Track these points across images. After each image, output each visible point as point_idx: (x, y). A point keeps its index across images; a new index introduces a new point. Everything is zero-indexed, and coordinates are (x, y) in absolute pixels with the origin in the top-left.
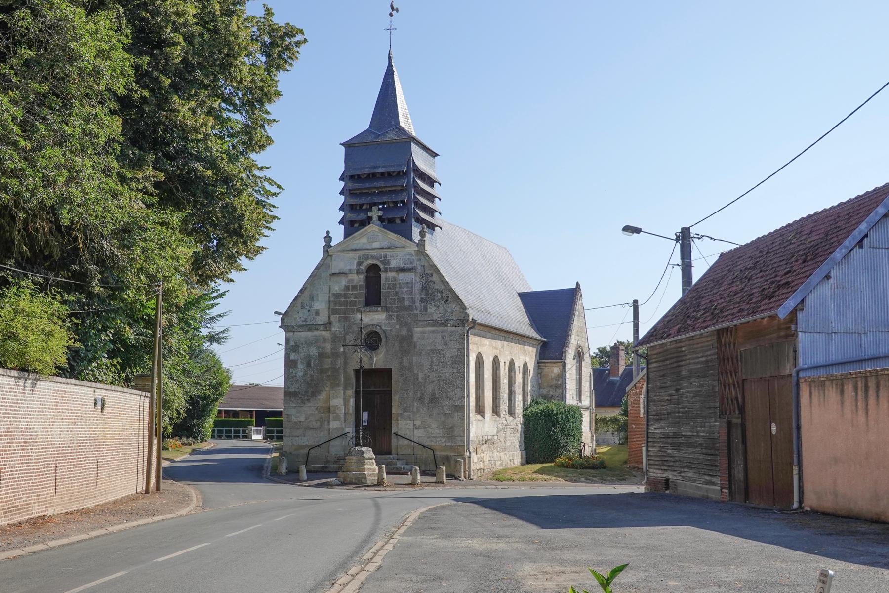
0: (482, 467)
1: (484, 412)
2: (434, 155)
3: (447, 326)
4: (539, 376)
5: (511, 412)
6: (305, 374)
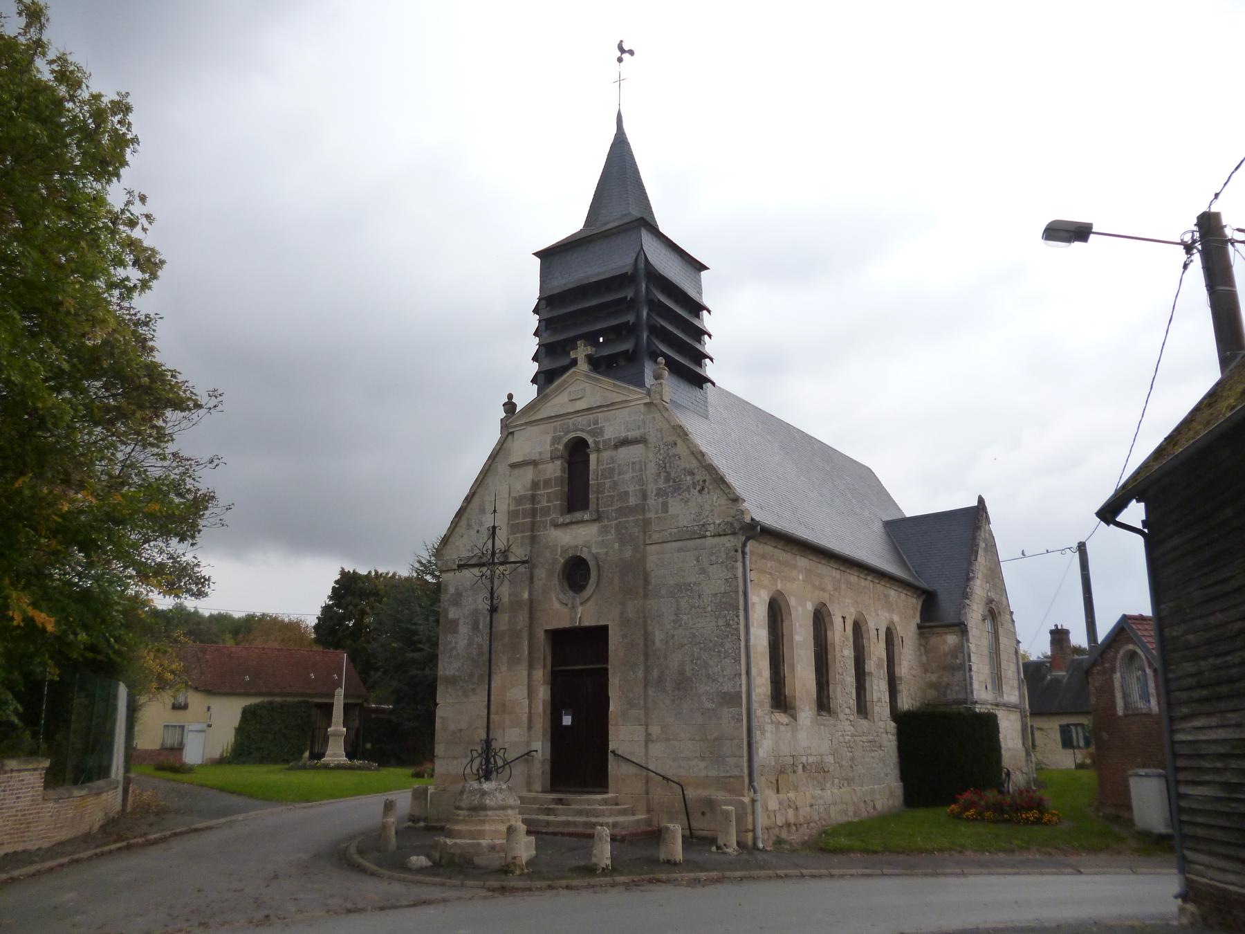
0: (791, 818)
1: (794, 708)
2: (698, 266)
3: (705, 537)
4: (923, 651)
5: (862, 708)
6: (470, 644)
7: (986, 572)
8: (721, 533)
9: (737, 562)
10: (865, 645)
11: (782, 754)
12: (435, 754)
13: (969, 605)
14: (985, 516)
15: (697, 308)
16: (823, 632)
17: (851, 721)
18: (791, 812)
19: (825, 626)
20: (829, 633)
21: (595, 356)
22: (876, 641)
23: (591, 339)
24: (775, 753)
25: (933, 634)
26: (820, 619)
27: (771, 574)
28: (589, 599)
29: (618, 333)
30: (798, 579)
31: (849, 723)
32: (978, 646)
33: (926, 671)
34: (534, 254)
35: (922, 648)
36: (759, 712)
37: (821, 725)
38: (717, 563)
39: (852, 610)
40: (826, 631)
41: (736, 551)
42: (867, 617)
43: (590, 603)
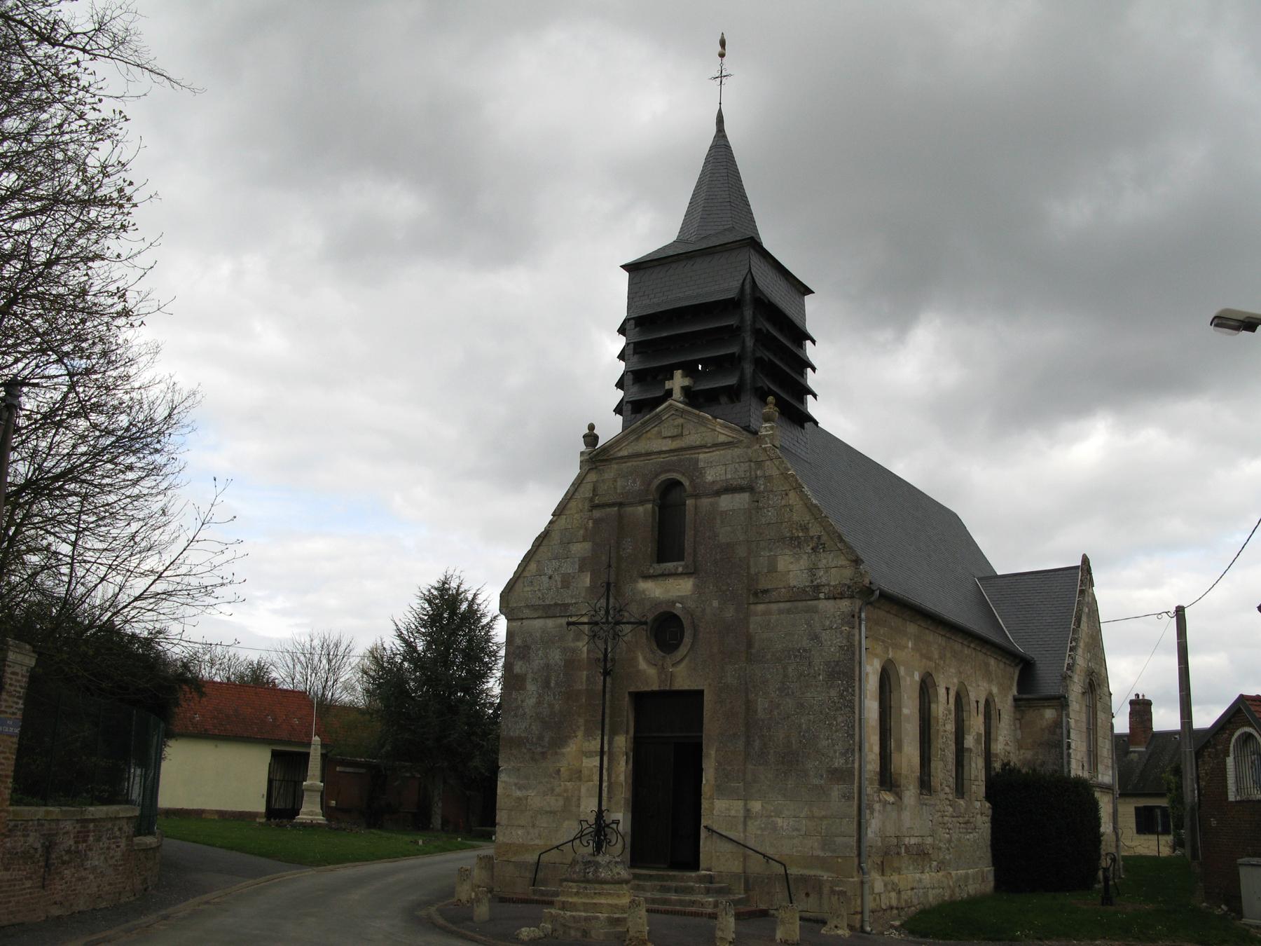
0: (894, 903)
1: (899, 786)
2: (802, 290)
3: (819, 599)
4: (1018, 726)
5: (960, 789)
6: (539, 703)
7: (1087, 640)
8: (837, 596)
9: (853, 628)
10: (965, 718)
11: (888, 834)
12: (497, 821)
13: (1071, 677)
14: (1089, 578)
15: (802, 336)
16: (927, 704)
17: (950, 801)
18: (893, 895)
19: (929, 697)
20: (933, 706)
21: (693, 389)
22: (976, 714)
23: (689, 369)
24: (882, 833)
25: (1030, 707)
26: (926, 689)
27: (883, 641)
28: (682, 660)
29: (720, 365)
30: (908, 647)
31: (948, 803)
32: (1076, 721)
33: (1020, 748)
34: (621, 266)
35: (1017, 722)
36: (869, 791)
37: (923, 804)
38: (831, 628)
39: (955, 680)
40: (929, 703)
41: (853, 616)
42: (969, 688)
43: (683, 664)
